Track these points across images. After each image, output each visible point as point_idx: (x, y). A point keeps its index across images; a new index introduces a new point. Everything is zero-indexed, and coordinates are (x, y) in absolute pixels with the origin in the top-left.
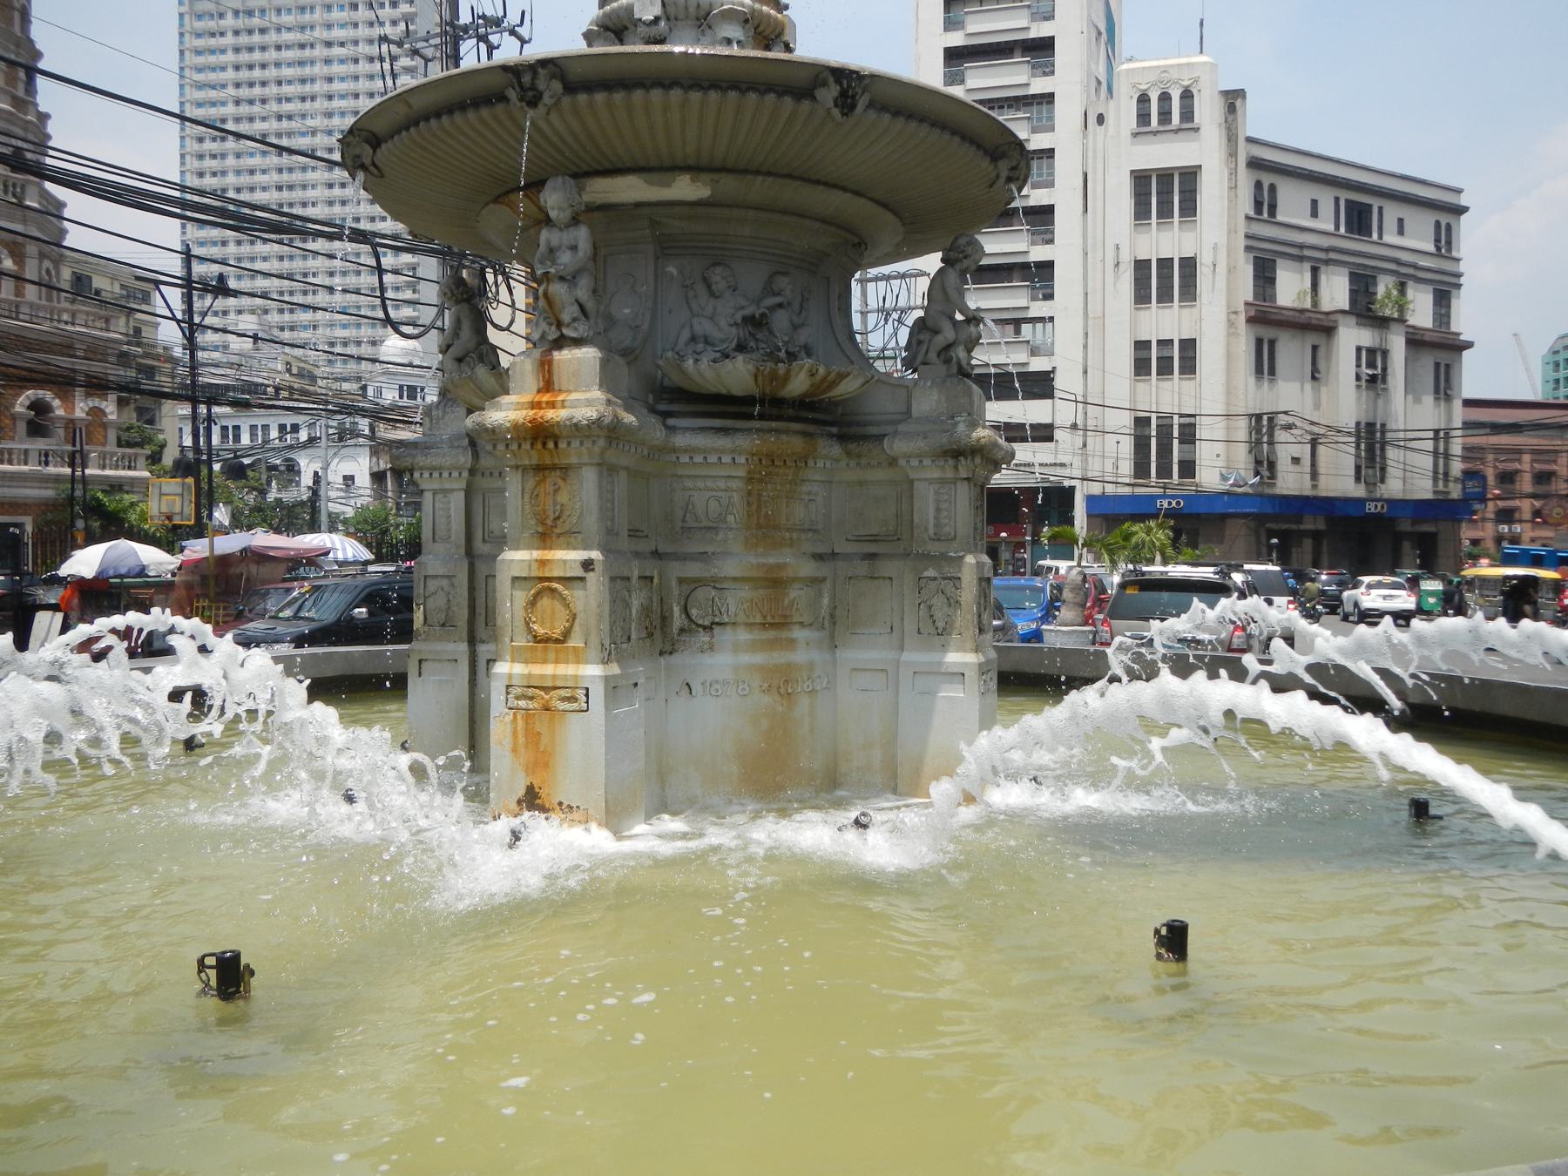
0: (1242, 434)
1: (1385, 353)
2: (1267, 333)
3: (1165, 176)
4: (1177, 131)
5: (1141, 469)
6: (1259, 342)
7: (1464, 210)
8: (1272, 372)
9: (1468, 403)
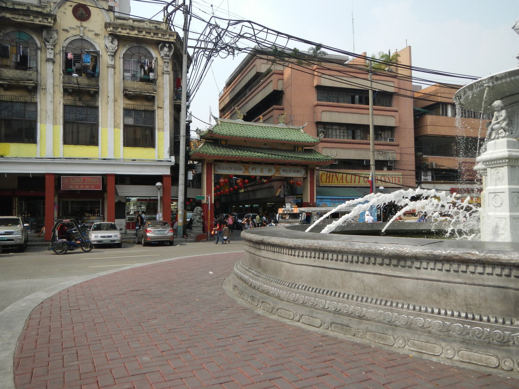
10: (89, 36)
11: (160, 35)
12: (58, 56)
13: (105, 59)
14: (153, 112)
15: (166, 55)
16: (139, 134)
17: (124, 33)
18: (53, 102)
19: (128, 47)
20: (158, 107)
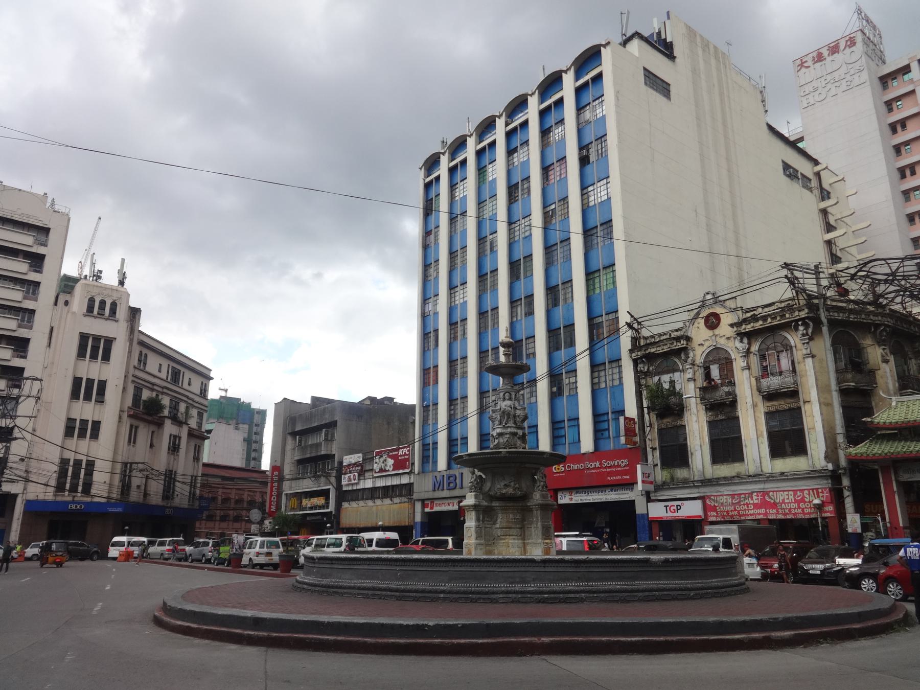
0: (118, 471)
1: (180, 438)
2: (136, 423)
3: (97, 339)
4: (107, 319)
5: (60, 488)
6: (131, 426)
7: (212, 378)
8: (134, 442)
9: (205, 465)
10: (722, 342)
11: (787, 316)
12: (698, 374)
13: (739, 363)
14: (800, 408)
15: (803, 335)
16: (787, 438)
17: (748, 328)
18: (698, 421)
19: (760, 340)
20: (805, 402)
